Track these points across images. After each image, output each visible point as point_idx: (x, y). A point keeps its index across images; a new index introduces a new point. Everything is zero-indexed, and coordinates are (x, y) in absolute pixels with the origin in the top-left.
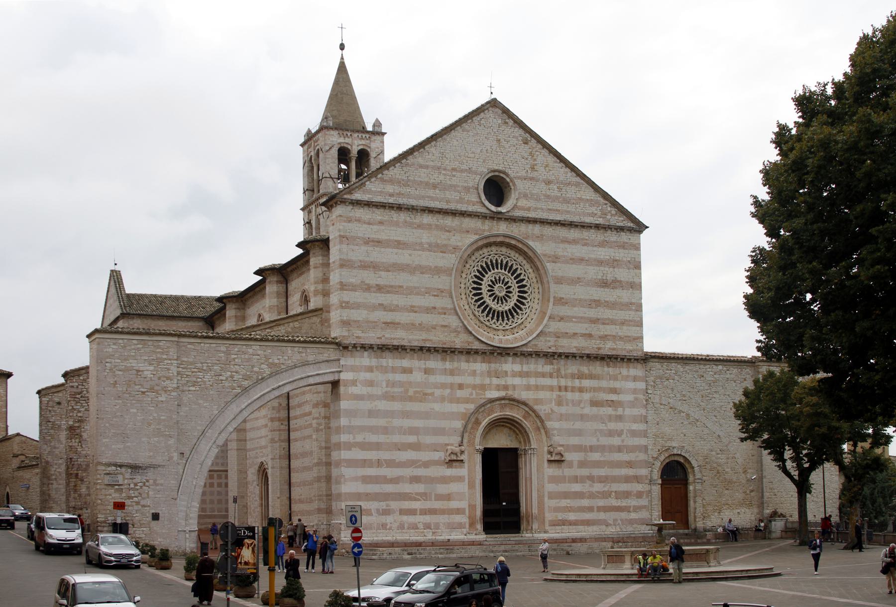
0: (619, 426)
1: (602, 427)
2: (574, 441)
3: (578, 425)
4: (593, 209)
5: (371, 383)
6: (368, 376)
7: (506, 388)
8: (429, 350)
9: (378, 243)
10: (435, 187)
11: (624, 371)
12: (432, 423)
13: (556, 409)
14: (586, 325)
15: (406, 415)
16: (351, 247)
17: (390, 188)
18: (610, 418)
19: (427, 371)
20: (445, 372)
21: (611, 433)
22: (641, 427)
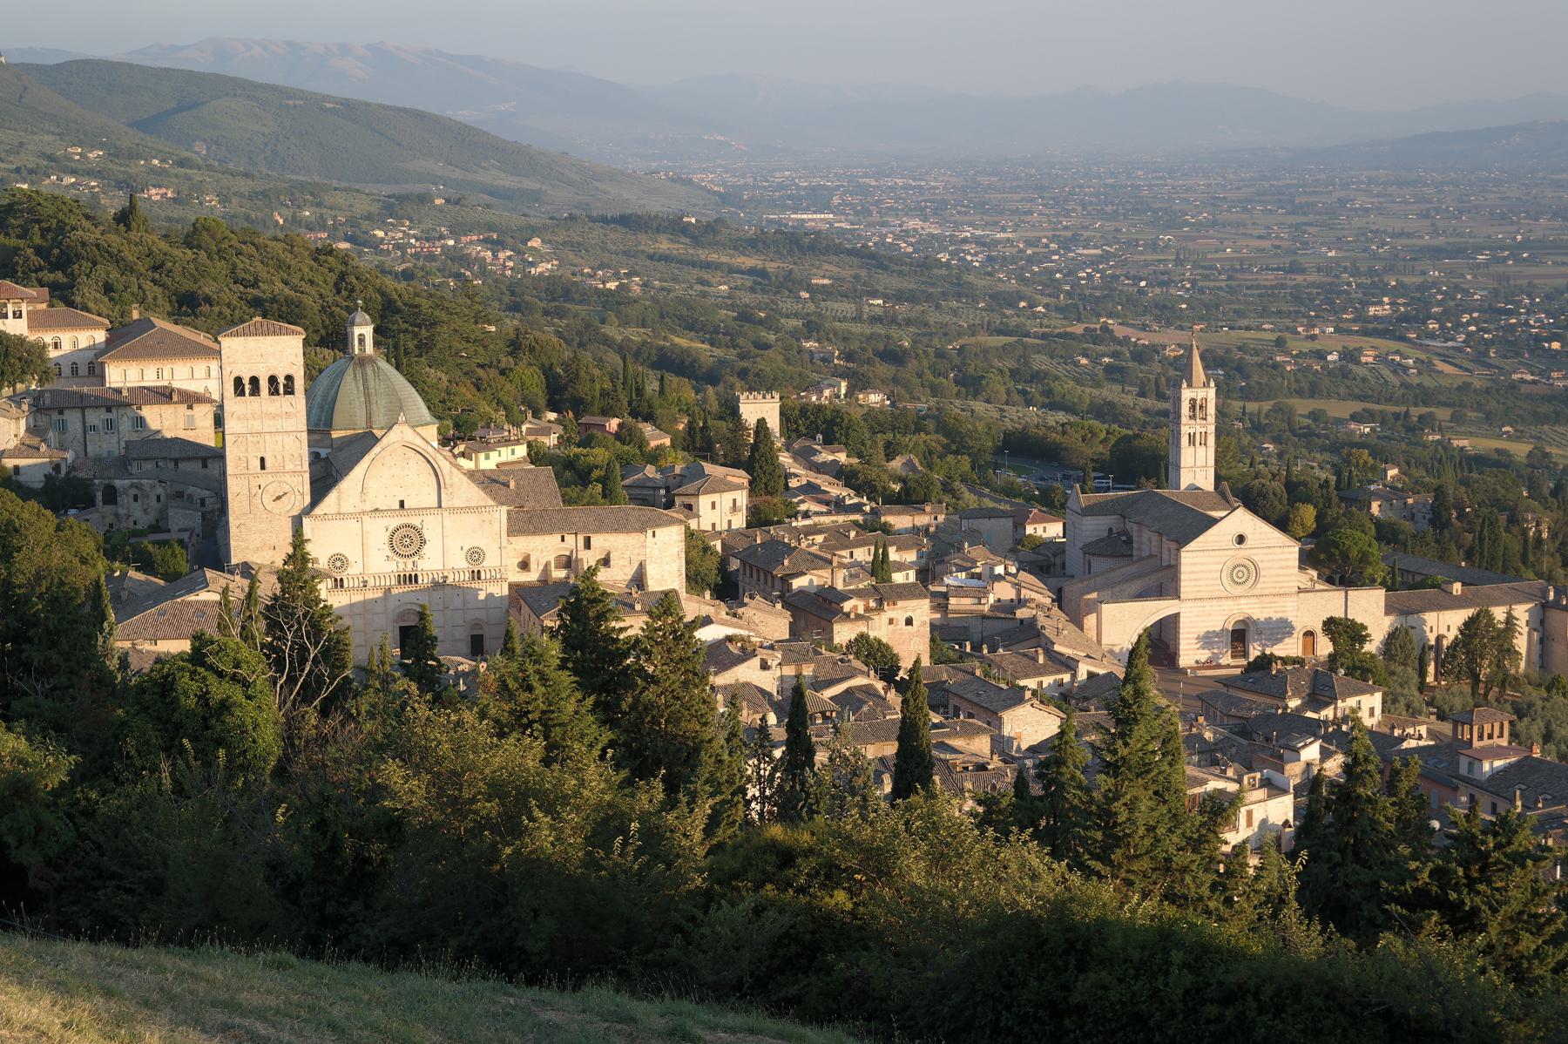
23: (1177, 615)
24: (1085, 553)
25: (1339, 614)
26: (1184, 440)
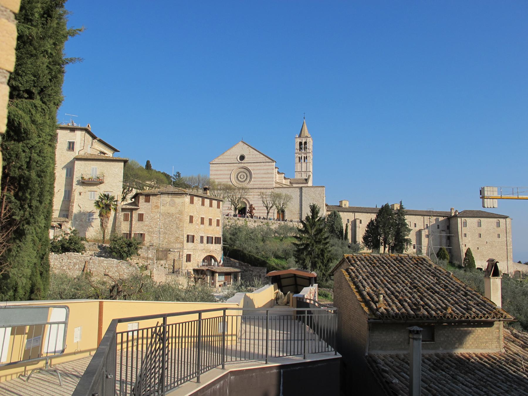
9: (217, 170)
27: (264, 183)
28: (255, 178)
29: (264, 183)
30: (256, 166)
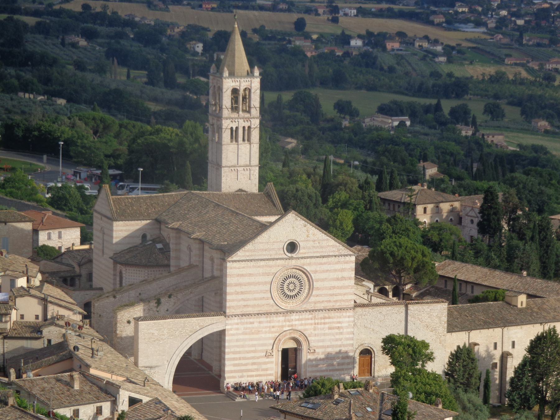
0: (341, 336)
1: (333, 337)
2: (321, 344)
3: (322, 338)
4: (334, 249)
5: (237, 329)
6: (236, 326)
7: (292, 326)
8: (261, 314)
9: (242, 275)
10: (266, 250)
11: (344, 314)
12: (261, 342)
13: (313, 332)
14: (328, 297)
15: (252, 340)
16: (232, 278)
17: (247, 254)
18: (337, 334)
19: (260, 322)
20: (267, 322)
21: (337, 340)
22: (351, 336)
23: (221, 334)
24: (116, 262)
25: (398, 330)
26: (226, 136)
27: (335, 298)
28: (318, 289)
29: (335, 298)
30: (321, 264)
